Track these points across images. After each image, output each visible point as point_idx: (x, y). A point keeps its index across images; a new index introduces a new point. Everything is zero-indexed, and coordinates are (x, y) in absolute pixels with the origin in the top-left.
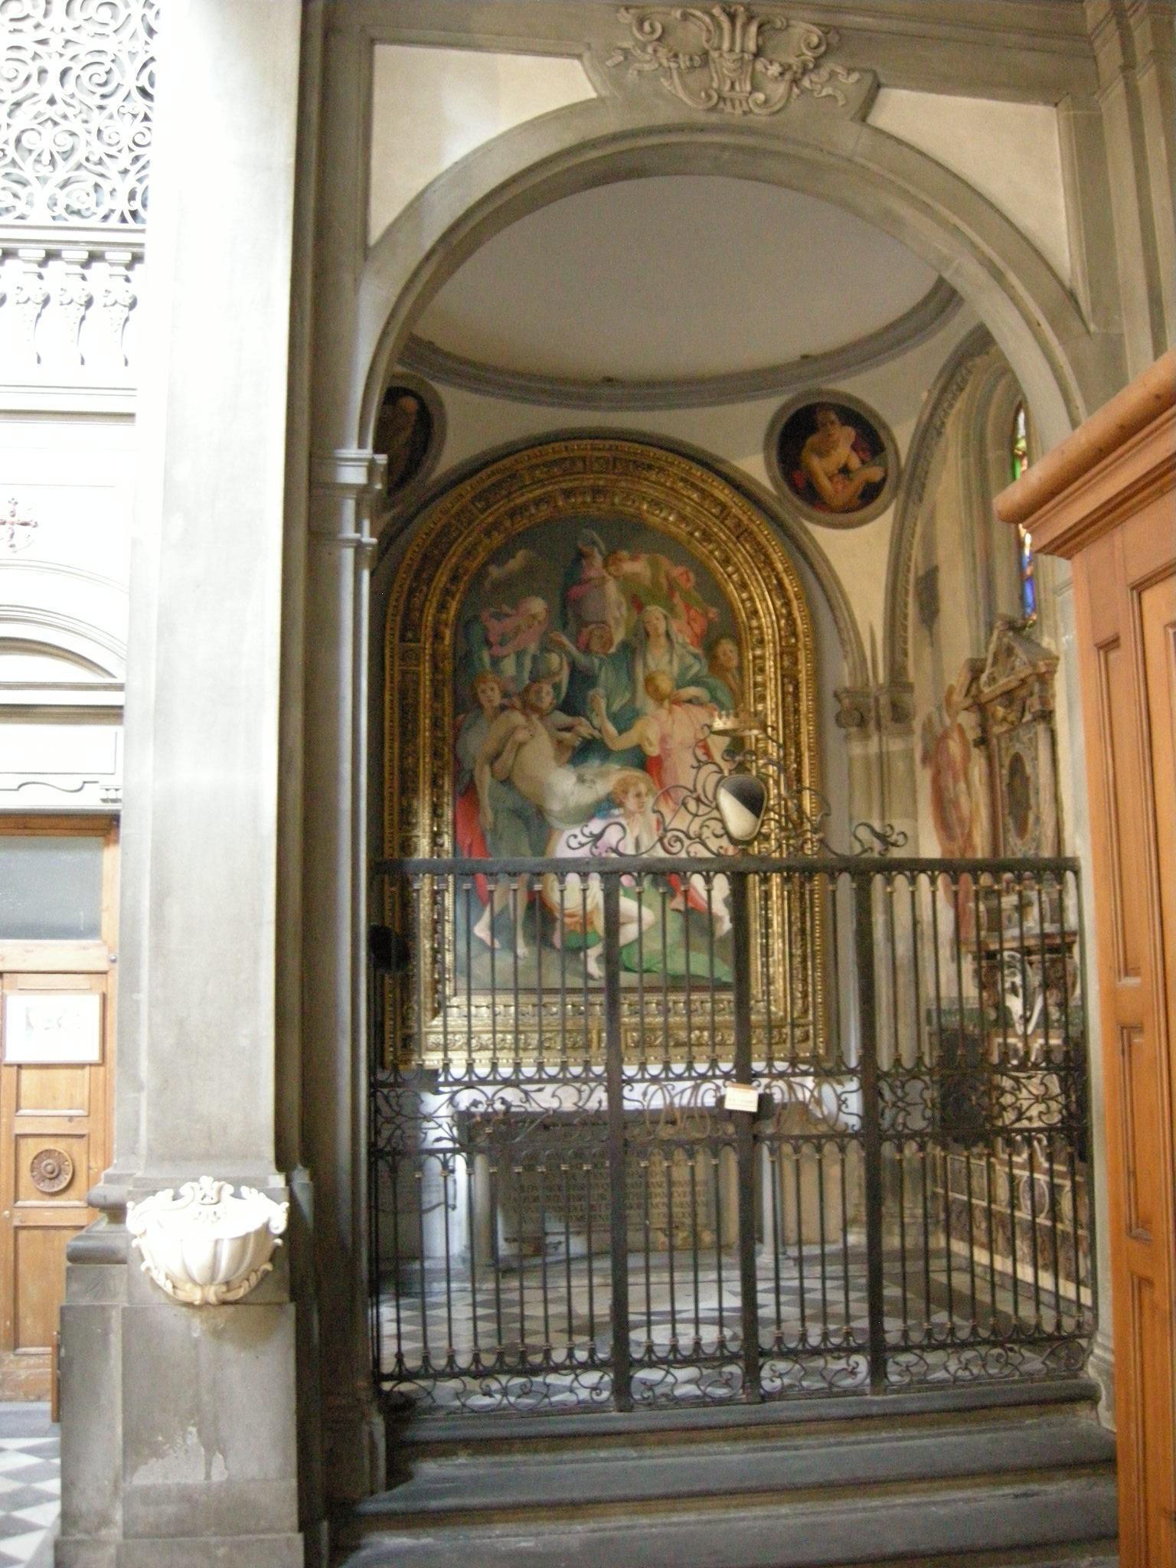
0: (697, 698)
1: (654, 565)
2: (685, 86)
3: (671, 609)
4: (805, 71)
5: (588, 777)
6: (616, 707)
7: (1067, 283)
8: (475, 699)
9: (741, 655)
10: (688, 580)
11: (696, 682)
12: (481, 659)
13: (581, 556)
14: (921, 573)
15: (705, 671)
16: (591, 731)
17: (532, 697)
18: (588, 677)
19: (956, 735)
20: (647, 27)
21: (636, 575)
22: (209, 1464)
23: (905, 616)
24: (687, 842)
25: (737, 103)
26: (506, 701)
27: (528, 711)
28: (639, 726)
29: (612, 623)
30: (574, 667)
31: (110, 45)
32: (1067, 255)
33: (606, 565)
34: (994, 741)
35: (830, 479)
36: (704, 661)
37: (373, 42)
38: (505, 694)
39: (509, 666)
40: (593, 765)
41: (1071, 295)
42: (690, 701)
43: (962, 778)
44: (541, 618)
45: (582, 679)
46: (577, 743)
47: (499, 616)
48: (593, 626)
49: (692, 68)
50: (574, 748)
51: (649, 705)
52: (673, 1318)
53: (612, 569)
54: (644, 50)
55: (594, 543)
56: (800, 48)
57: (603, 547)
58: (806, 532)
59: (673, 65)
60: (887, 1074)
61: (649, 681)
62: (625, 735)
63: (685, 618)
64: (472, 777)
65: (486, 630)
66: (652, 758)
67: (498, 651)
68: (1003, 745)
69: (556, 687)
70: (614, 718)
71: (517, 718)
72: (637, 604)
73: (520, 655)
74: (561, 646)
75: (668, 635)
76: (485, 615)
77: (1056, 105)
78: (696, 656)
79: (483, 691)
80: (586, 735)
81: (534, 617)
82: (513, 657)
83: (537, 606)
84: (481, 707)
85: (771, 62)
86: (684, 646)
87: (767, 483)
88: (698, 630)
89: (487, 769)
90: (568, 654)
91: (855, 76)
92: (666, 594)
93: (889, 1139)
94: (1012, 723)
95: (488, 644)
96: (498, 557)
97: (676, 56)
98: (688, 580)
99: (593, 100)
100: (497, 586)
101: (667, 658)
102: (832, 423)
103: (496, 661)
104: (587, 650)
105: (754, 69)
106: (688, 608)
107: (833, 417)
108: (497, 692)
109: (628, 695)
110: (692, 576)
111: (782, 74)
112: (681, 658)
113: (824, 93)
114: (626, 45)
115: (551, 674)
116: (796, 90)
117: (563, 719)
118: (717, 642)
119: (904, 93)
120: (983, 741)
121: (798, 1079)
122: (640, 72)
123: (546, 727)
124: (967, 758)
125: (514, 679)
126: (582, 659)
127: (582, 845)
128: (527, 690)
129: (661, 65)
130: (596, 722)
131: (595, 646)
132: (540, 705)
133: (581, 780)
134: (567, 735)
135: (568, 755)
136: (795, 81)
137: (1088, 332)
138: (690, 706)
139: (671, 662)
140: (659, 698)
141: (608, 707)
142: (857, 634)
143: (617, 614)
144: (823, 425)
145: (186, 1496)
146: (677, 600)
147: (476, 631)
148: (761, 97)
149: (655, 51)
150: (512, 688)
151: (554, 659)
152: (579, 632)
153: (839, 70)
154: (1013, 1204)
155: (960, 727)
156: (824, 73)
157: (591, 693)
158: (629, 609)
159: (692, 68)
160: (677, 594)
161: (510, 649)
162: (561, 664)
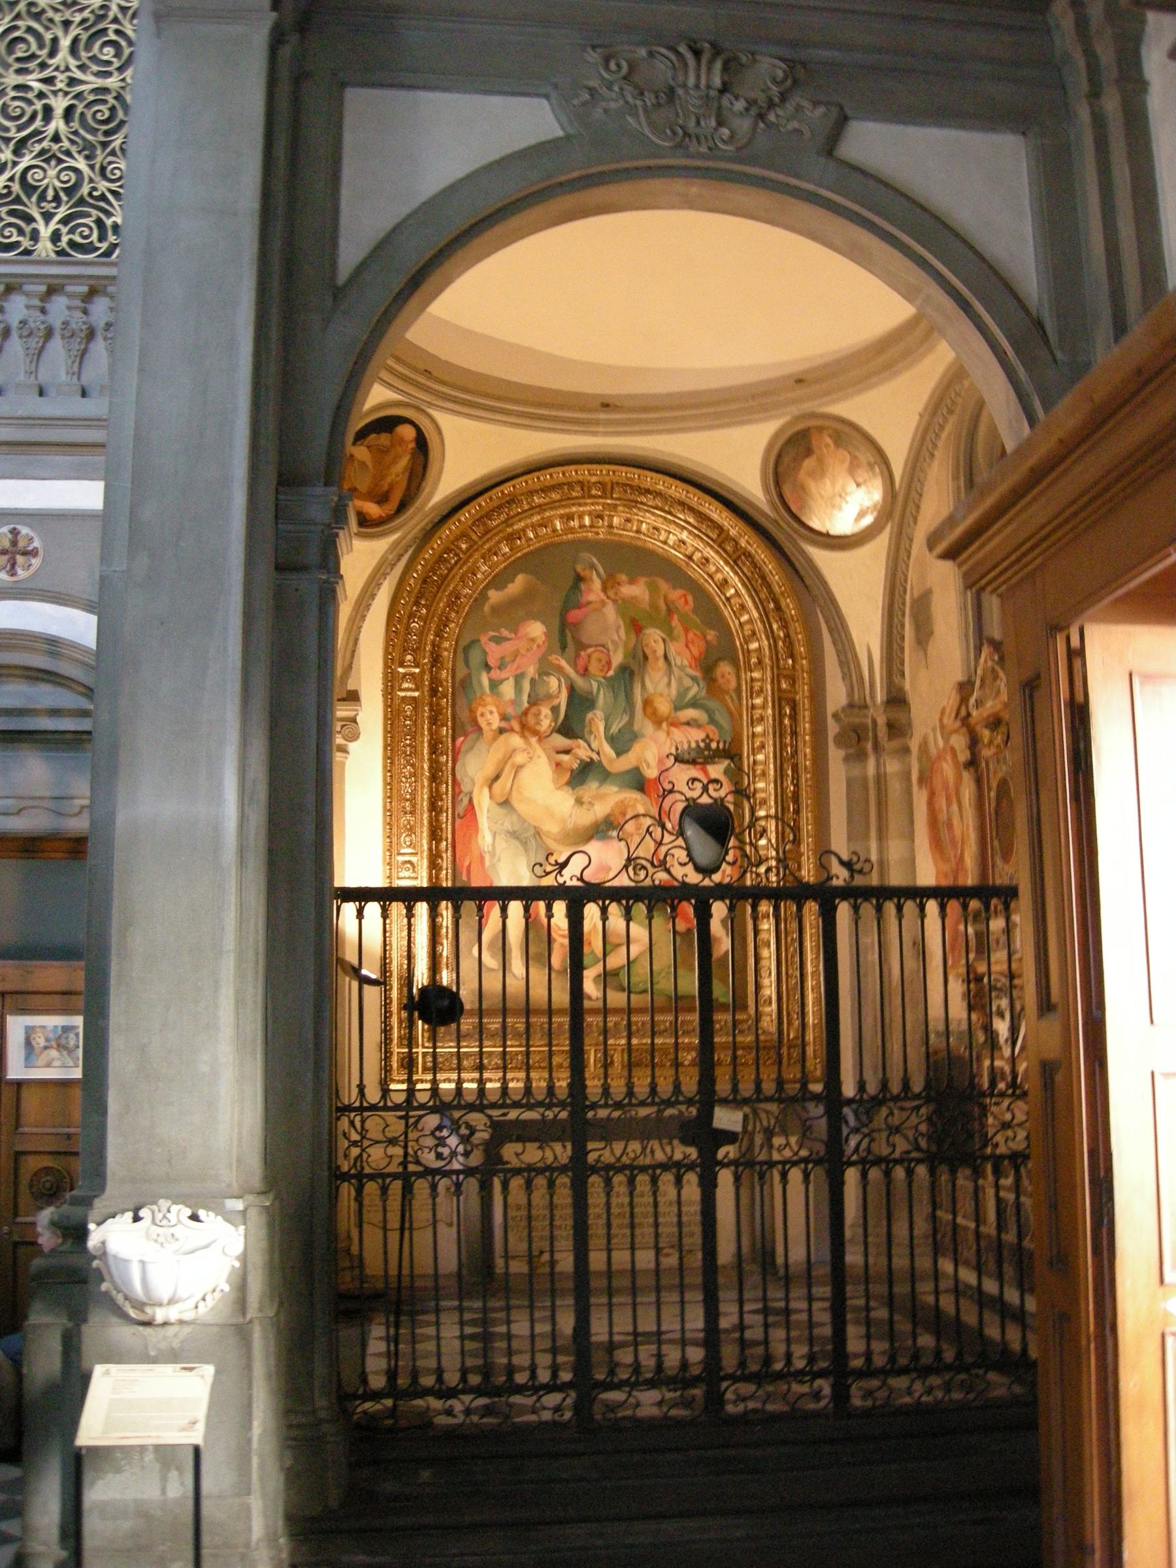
0: (695, 721)
1: (653, 589)
2: (650, 124)
3: (670, 632)
4: (771, 105)
5: (585, 799)
6: (614, 729)
7: (1034, 313)
8: (475, 722)
9: (738, 678)
10: (686, 602)
11: (694, 704)
13: (579, 579)
14: (916, 595)
15: (703, 693)
16: (590, 753)
17: (531, 720)
18: (588, 700)
19: (949, 758)
20: (613, 66)
21: (634, 598)
22: (164, 1479)
23: (903, 638)
24: (651, 870)
25: (703, 139)
26: (504, 724)
27: (527, 734)
28: (637, 748)
29: (611, 647)
30: (572, 690)
31: (112, 82)
32: (1035, 285)
34: (983, 764)
36: (702, 684)
37: (343, 85)
38: (504, 717)
39: (508, 690)
40: (592, 787)
41: (1039, 324)
42: (688, 724)
43: (954, 800)
44: (540, 641)
45: (580, 702)
46: (575, 766)
47: (498, 640)
48: (590, 650)
49: (659, 105)
50: (572, 771)
51: (648, 728)
52: (658, 1336)
53: (611, 593)
54: (610, 88)
55: (592, 567)
56: (765, 83)
58: (803, 553)
59: (639, 103)
60: (850, 1102)
61: (647, 703)
62: (623, 758)
63: (683, 638)
64: (471, 801)
65: (486, 653)
66: (649, 780)
67: (495, 674)
68: (991, 766)
69: (555, 710)
70: (612, 740)
71: (516, 740)
72: (636, 627)
73: (518, 679)
74: (560, 669)
75: (666, 657)
76: (484, 639)
77: (1024, 134)
78: (694, 679)
79: (482, 715)
81: (533, 640)
82: (511, 681)
83: (536, 630)
84: (480, 729)
85: (737, 98)
86: (682, 668)
87: (766, 508)
88: (696, 652)
89: (486, 791)
90: (567, 677)
91: (821, 110)
92: (664, 617)
93: (850, 1164)
94: (998, 746)
95: (488, 667)
96: (499, 581)
97: (642, 94)
98: (686, 602)
99: (561, 139)
100: (497, 610)
101: (666, 680)
102: (827, 445)
103: (495, 685)
104: (585, 673)
105: (720, 108)
106: (686, 631)
107: (829, 440)
108: (496, 715)
109: (626, 718)
110: (690, 598)
111: (747, 110)
112: (680, 681)
113: (790, 127)
114: (591, 83)
115: (549, 697)
116: (762, 125)
117: (560, 741)
118: (715, 663)
119: (871, 125)
120: (973, 763)
121: (763, 1105)
122: (606, 111)
123: (544, 750)
124: (959, 778)
126: (580, 682)
127: (547, 874)
128: (526, 713)
129: (627, 102)
130: (594, 746)
131: (594, 667)
132: (538, 728)
133: (579, 802)
134: (565, 758)
135: (567, 776)
136: (761, 116)
137: (1055, 360)
138: (687, 728)
139: (669, 684)
140: (658, 721)
141: (607, 728)
142: (856, 656)
143: (616, 638)
145: (142, 1511)
146: (675, 622)
147: (475, 656)
148: (725, 132)
149: (622, 89)
150: (510, 711)
151: (553, 682)
152: (577, 656)
153: (805, 104)
154: (1001, 1226)
155: (953, 750)
156: (790, 106)
157: (590, 715)
158: (627, 633)
159: (659, 105)
160: (676, 617)
161: (508, 673)
162: (560, 686)
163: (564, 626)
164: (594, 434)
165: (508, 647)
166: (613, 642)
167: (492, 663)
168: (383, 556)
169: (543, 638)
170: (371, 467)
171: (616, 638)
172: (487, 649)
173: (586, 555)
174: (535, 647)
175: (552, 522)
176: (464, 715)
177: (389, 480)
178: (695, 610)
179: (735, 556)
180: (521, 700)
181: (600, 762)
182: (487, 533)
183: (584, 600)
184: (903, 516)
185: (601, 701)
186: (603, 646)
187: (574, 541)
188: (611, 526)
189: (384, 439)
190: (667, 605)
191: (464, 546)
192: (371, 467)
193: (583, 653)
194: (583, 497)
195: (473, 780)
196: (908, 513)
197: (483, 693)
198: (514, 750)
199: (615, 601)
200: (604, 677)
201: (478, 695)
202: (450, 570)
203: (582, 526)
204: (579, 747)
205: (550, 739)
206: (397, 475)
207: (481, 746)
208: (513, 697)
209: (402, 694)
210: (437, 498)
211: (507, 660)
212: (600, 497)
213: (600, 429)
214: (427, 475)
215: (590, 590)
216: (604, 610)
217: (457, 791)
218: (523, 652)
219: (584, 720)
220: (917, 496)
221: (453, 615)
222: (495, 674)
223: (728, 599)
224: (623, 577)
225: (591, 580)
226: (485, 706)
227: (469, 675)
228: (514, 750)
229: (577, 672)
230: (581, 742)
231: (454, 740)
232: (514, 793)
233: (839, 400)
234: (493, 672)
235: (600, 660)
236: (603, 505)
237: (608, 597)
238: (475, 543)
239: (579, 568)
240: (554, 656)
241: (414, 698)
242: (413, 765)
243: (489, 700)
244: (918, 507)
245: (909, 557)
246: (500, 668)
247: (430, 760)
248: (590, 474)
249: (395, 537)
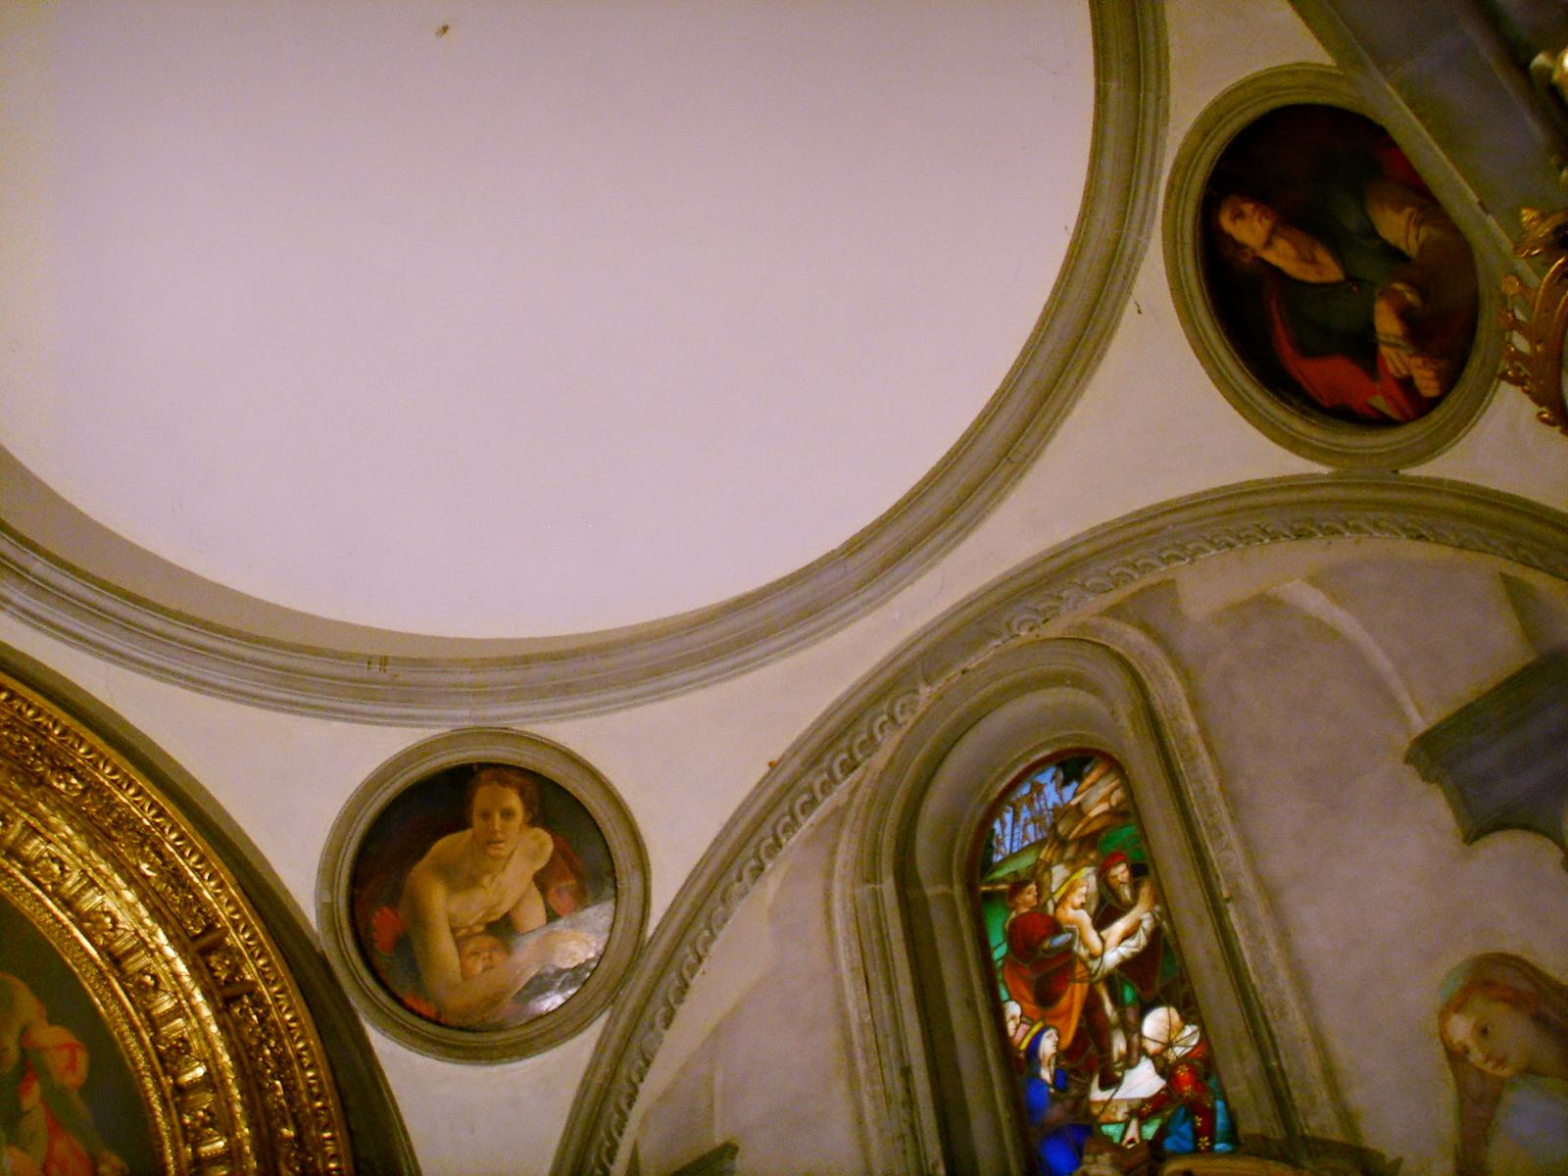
10: (72, 1066)
35: (459, 943)
98: (72, 1066)
102: (507, 814)
106: (55, 1127)
107: (514, 802)
110: (82, 1059)
144: (486, 815)
160: (36, 1089)
178: (85, 1089)
179: (229, 991)
184: (649, 996)
190: (23, 1050)
196: (658, 1001)
220: (692, 959)
223: (179, 1089)
233: (575, 712)
244: (685, 986)
245: (630, 1105)
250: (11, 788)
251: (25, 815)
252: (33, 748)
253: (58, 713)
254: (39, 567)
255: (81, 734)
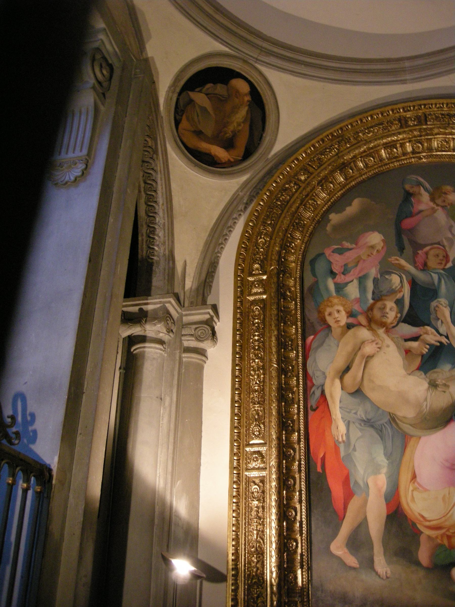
5: (439, 382)
8: (324, 321)
12: (327, 289)
13: (408, 196)
16: (439, 338)
17: (377, 314)
26: (351, 320)
27: (374, 326)
29: (446, 243)
30: (414, 283)
33: (433, 199)
38: (351, 314)
44: (379, 247)
46: (425, 351)
47: (341, 251)
48: (428, 248)
50: (423, 356)
53: (439, 201)
55: (419, 184)
57: (428, 186)
64: (323, 392)
65: (330, 263)
67: (340, 279)
69: (399, 302)
73: (362, 280)
74: (401, 268)
76: (328, 252)
79: (330, 314)
80: (433, 342)
81: (372, 247)
82: (356, 282)
84: (329, 327)
90: (407, 273)
95: (333, 274)
100: (338, 228)
103: (340, 288)
104: (425, 267)
108: (343, 313)
115: (393, 292)
125: (358, 301)
126: (421, 276)
128: (371, 308)
130: (442, 330)
131: (432, 263)
132: (384, 320)
133: (433, 385)
134: (414, 344)
135: (418, 361)
143: (450, 236)
147: (321, 267)
150: (356, 308)
151: (395, 279)
152: (415, 254)
157: (434, 304)
161: (353, 276)
163: (399, 233)
164: (404, 82)
165: (350, 256)
166: (448, 239)
167: (336, 269)
168: (234, 194)
169: (382, 244)
170: (211, 112)
171: (450, 236)
172: (331, 261)
173: (414, 177)
174: (375, 252)
175: (378, 152)
176: (313, 316)
177: (231, 128)
180: (366, 297)
181: (450, 345)
182: (322, 165)
183: (415, 210)
185: (443, 289)
186: (439, 243)
187: (402, 166)
188: (430, 149)
189: (220, 89)
191: (303, 178)
192: (211, 112)
193: (420, 252)
194: (401, 127)
195: (324, 373)
197: (330, 296)
198: (363, 343)
199: (443, 207)
200: (443, 269)
201: (325, 298)
202: (291, 198)
203: (404, 154)
204: (427, 333)
205: (397, 328)
206: (239, 125)
207: (331, 341)
208: (358, 296)
209: (251, 298)
210: (278, 147)
211: (350, 266)
212: (416, 125)
213: (408, 77)
214: (267, 128)
215: (419, 202)
216: (435, 215)
217: (309, 383)
218: (364, 257)
219: (428, 308)
221: (298, 235)
222: (340, 279)
224: (449, 188)
225: (420, 194)
226: (332, 306)
227: (317, 282)
228: (363, 343)
229: (416, 267)
230: (428, 328)
231: (304, 339)
232: (366, 382)
234: (337, 277)
235: (438, 255)
236: (420, 130)
237: (438, 205)
238: (312, 174)
239: (407, 187)
240: (393, 258)
241: (263, 300)
242: (262, 359)
243: (336, 301)
246: (344, 273)
247: (278, 352)
248: (405, 111)
249: (244, 178)
250: (441, 131)
251: (451, 136)
252: (440, 116)
253: (441, 101)
254: (407, 64)
255: (453, 102)
